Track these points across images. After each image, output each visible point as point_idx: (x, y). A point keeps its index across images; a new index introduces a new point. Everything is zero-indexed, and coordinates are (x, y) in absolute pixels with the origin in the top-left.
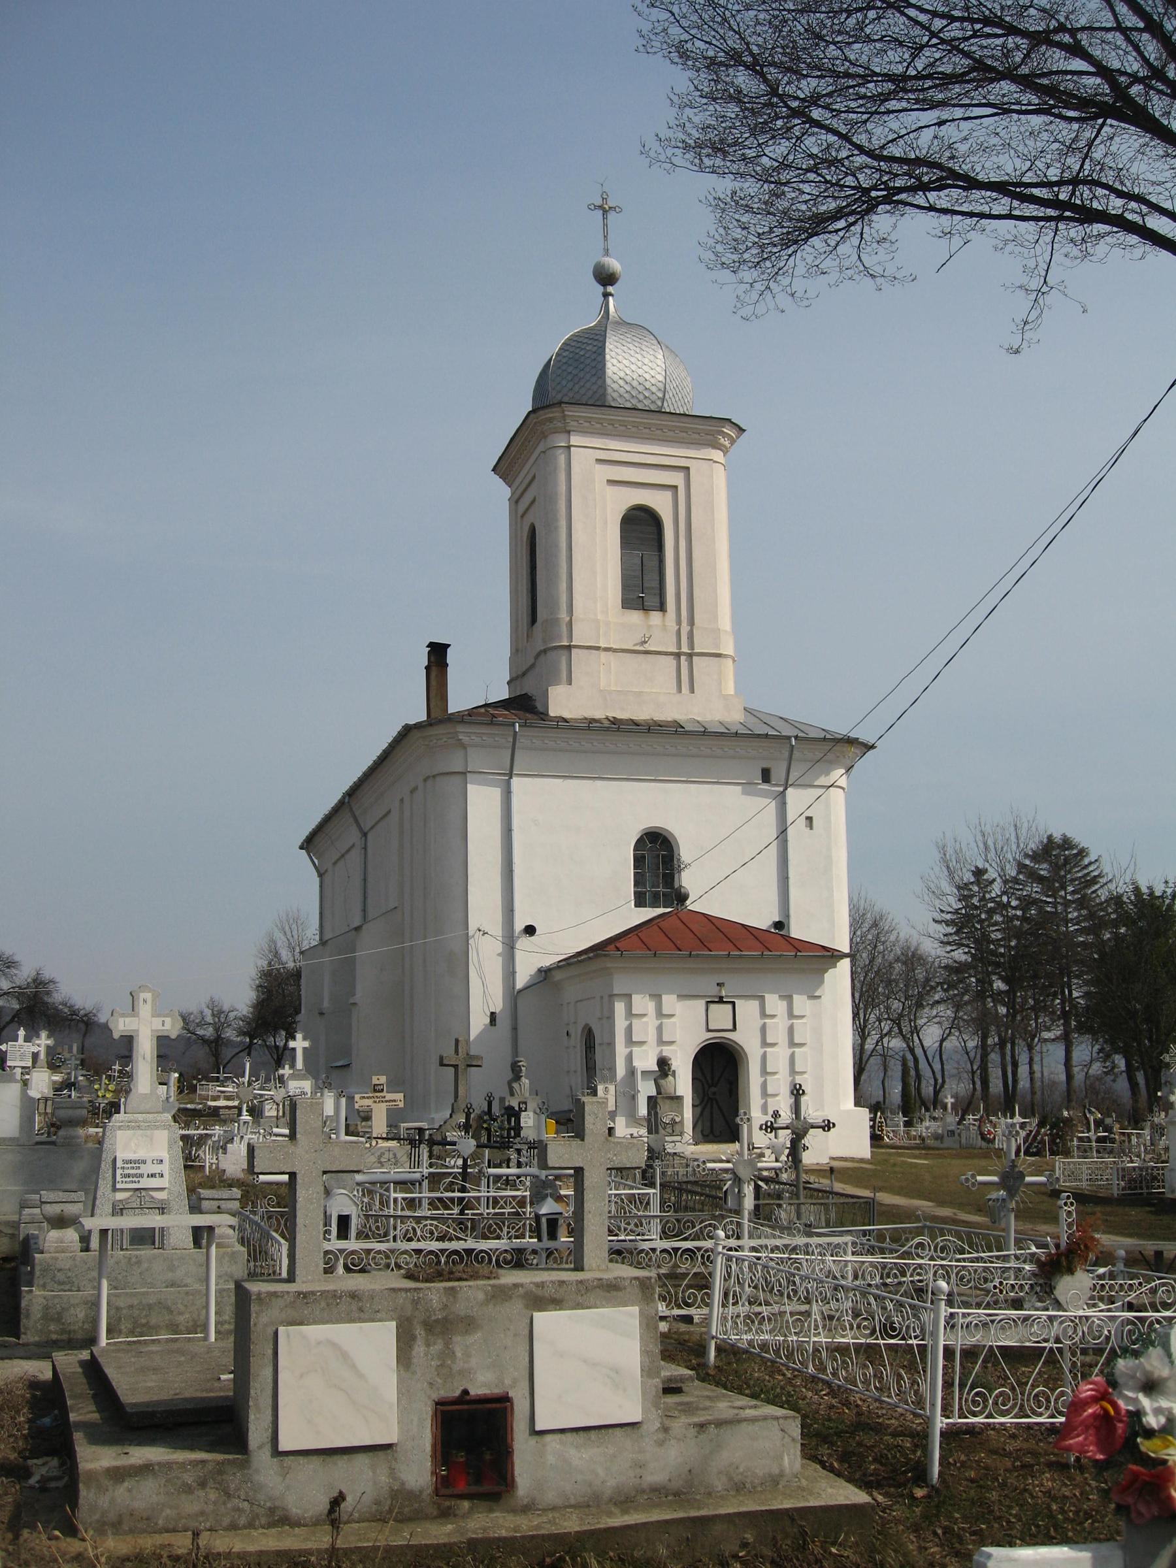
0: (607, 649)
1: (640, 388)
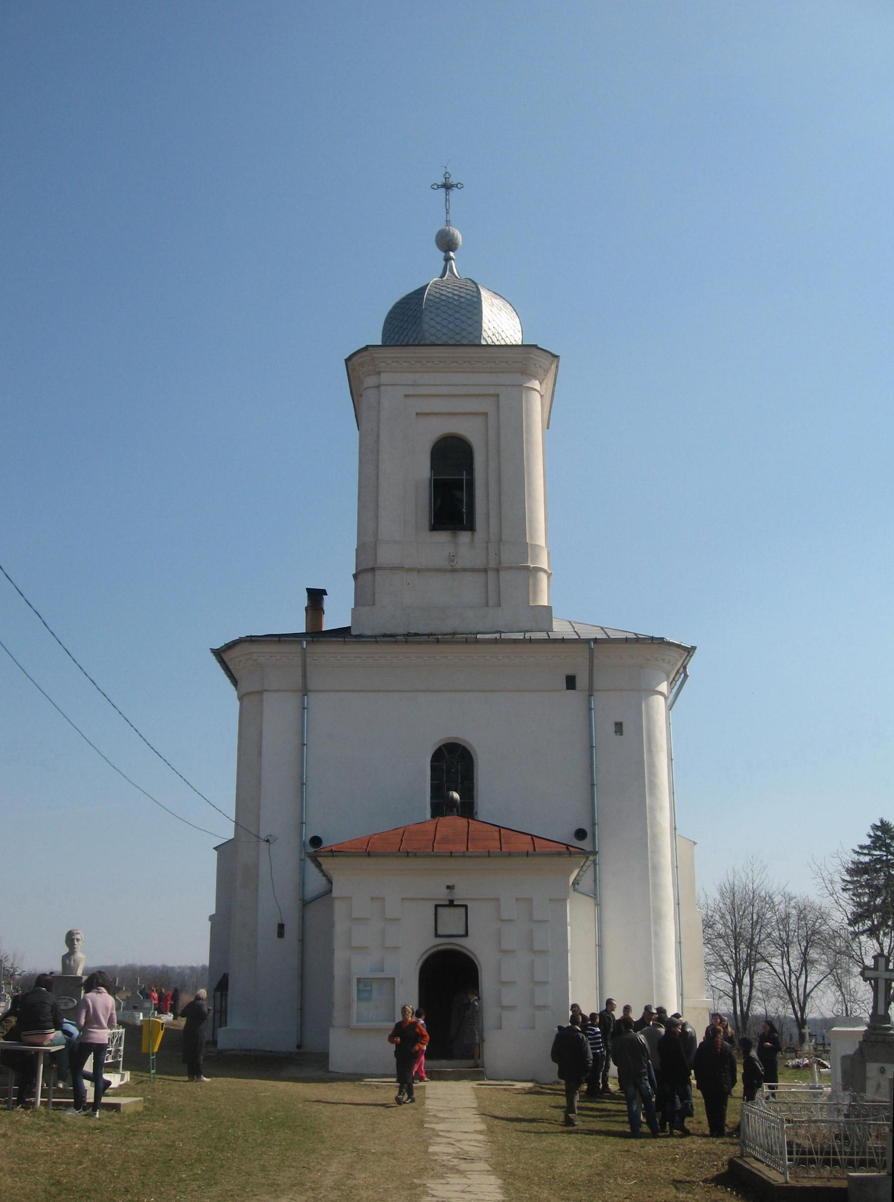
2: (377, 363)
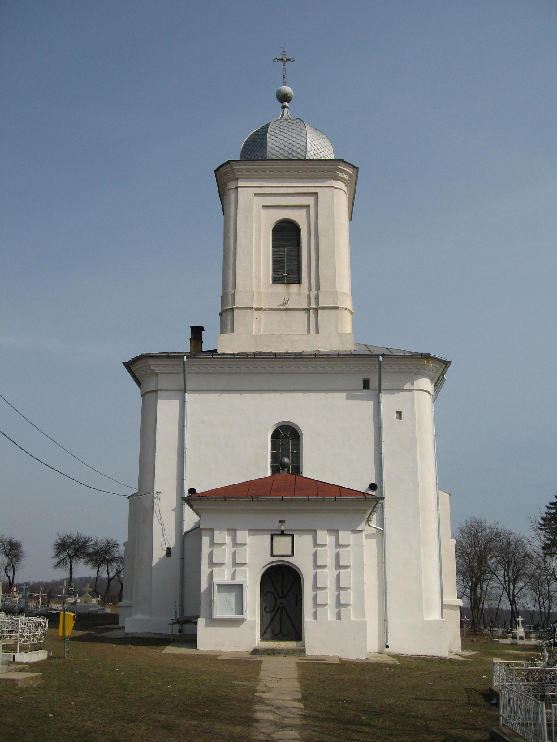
0: (258, 309)
1: (290, 151)
2: (235, 172)
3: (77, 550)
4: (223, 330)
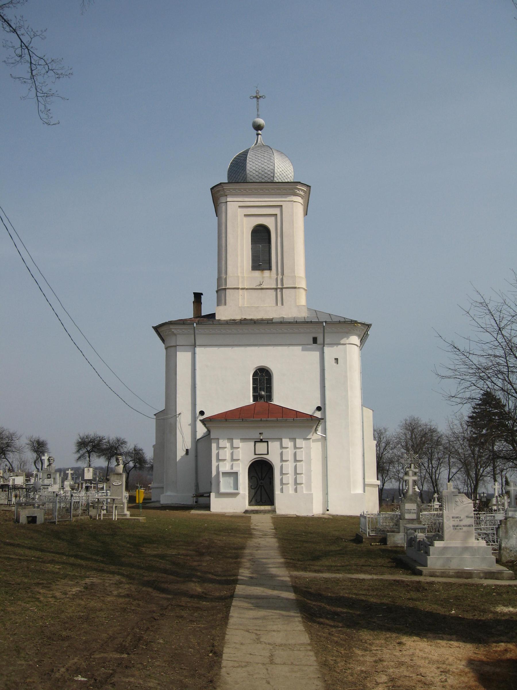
1: (263, 173)
3: (94, 447)
4: (219, 304)
